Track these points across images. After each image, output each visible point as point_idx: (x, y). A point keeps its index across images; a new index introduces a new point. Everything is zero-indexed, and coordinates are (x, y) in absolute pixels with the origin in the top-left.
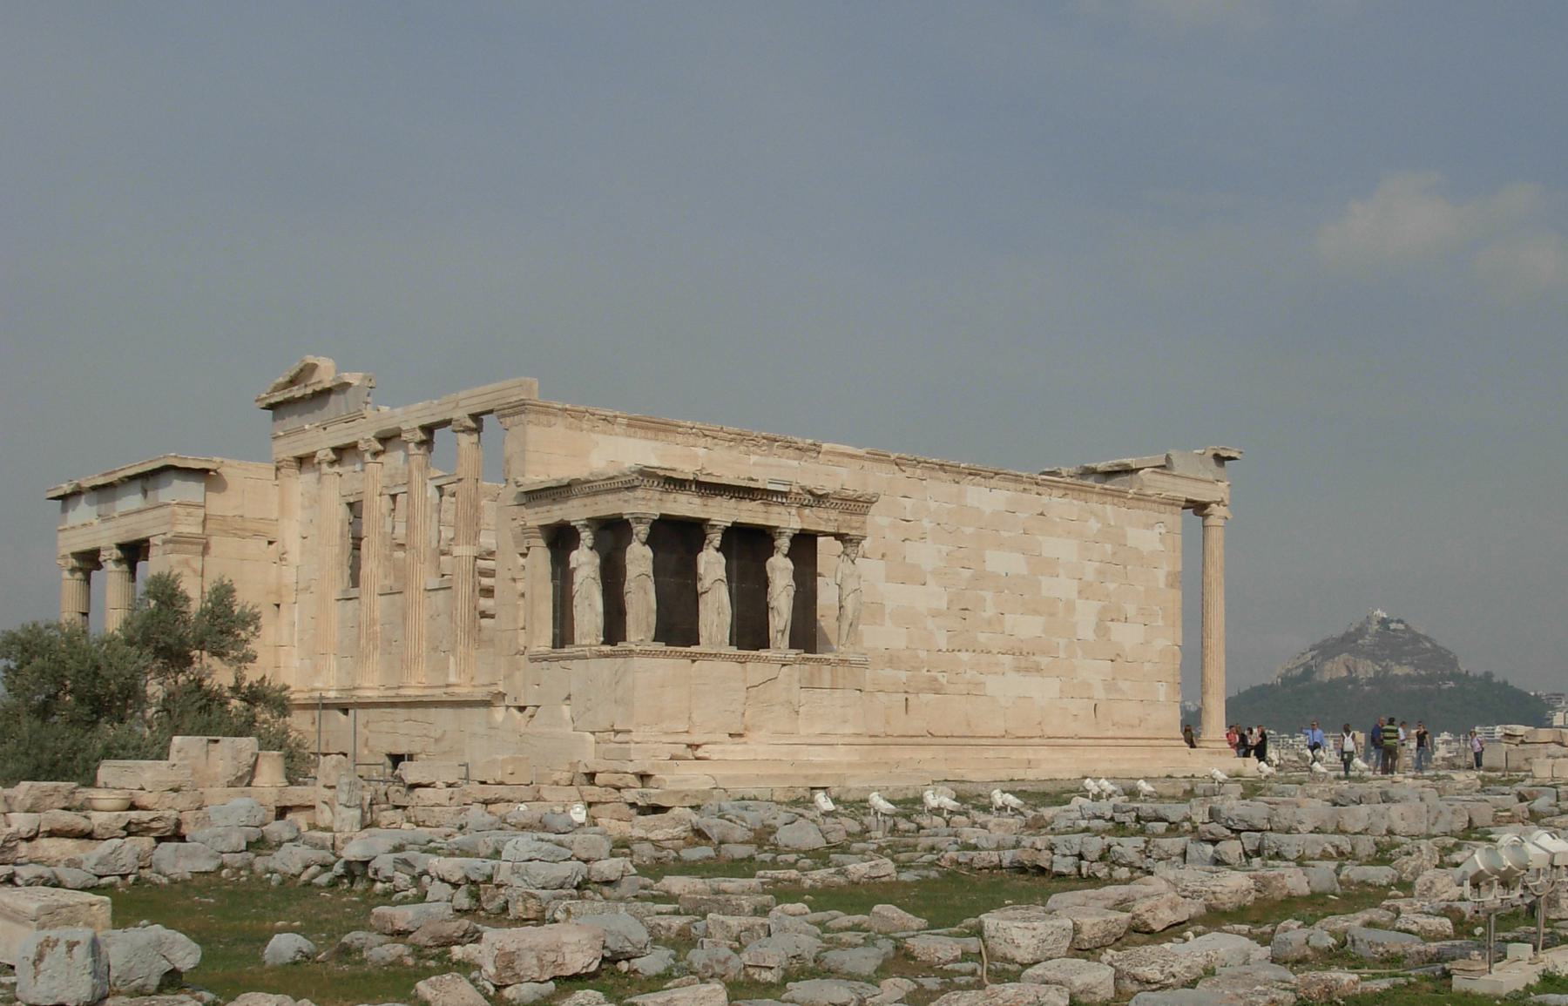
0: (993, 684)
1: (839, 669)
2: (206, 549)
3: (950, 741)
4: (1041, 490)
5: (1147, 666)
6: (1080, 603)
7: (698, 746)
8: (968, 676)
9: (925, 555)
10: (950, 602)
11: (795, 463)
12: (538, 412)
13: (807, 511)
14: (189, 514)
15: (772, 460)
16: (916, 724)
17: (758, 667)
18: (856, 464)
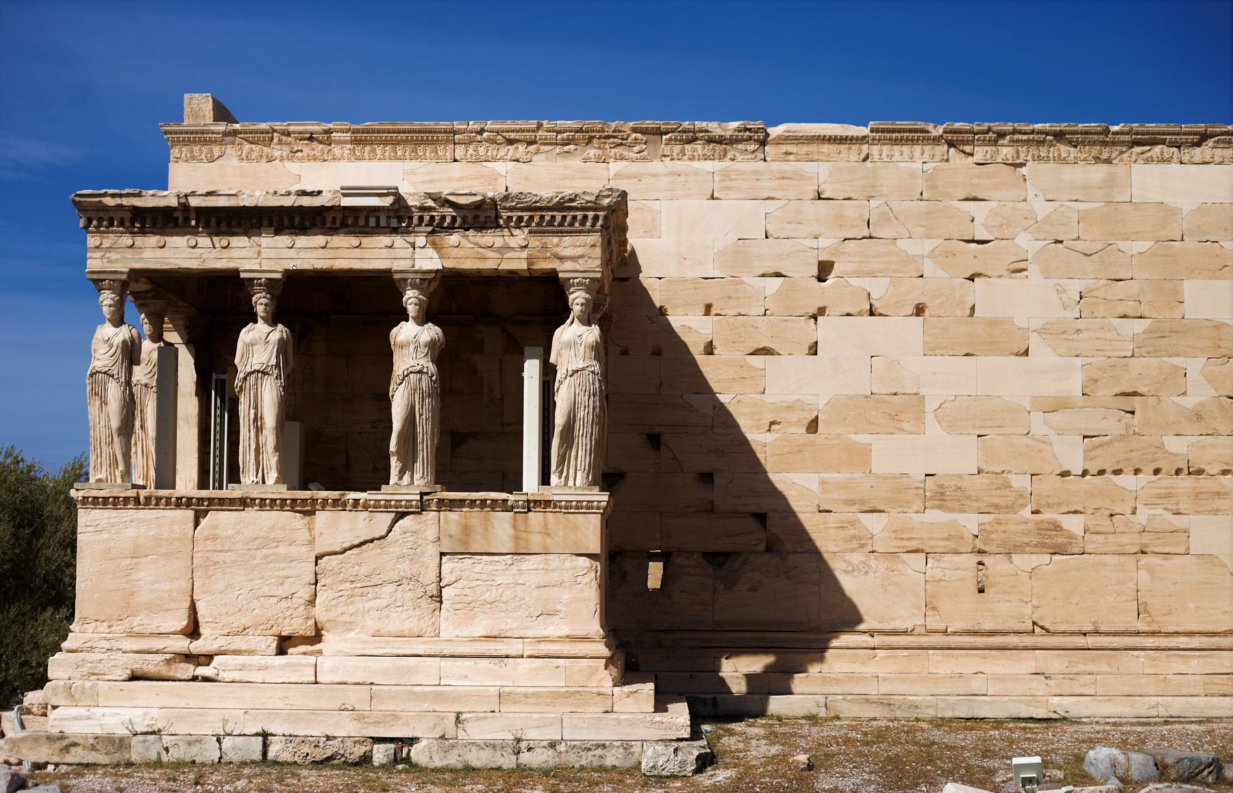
1: (535, 517)
3: (1090, 641)
9: (1026, 301)
11: (709, 165)
12: (188, 142)
13: (454, 238)
15: (656, 166)
16: (1002, 611)
18: (852, 154)
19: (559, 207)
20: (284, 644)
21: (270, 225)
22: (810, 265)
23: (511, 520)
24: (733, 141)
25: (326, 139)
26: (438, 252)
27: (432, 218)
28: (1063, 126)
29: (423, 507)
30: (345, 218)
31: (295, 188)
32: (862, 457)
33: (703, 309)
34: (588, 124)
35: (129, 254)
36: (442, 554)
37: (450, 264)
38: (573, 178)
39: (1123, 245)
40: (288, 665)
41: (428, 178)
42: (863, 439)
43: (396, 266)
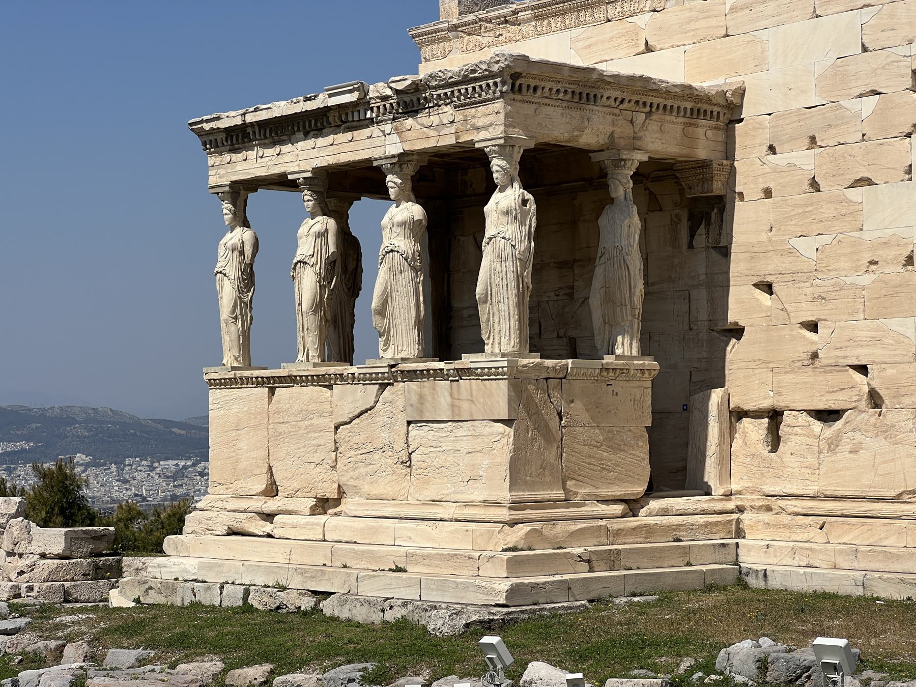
13: (409, 122)
19: (466, 80)
20: (323, 505)
21: (299, 130)
22: (903, 76)
23: (448, 388)
26: (400, 137)
27: (391, 104)
30: (340, 116)
33: (807, 141)
35: (229, 168)
36: (409, 423)
38: (697, 19)
40: (307, 524)
41: (588, 43)
43: (376, 153)
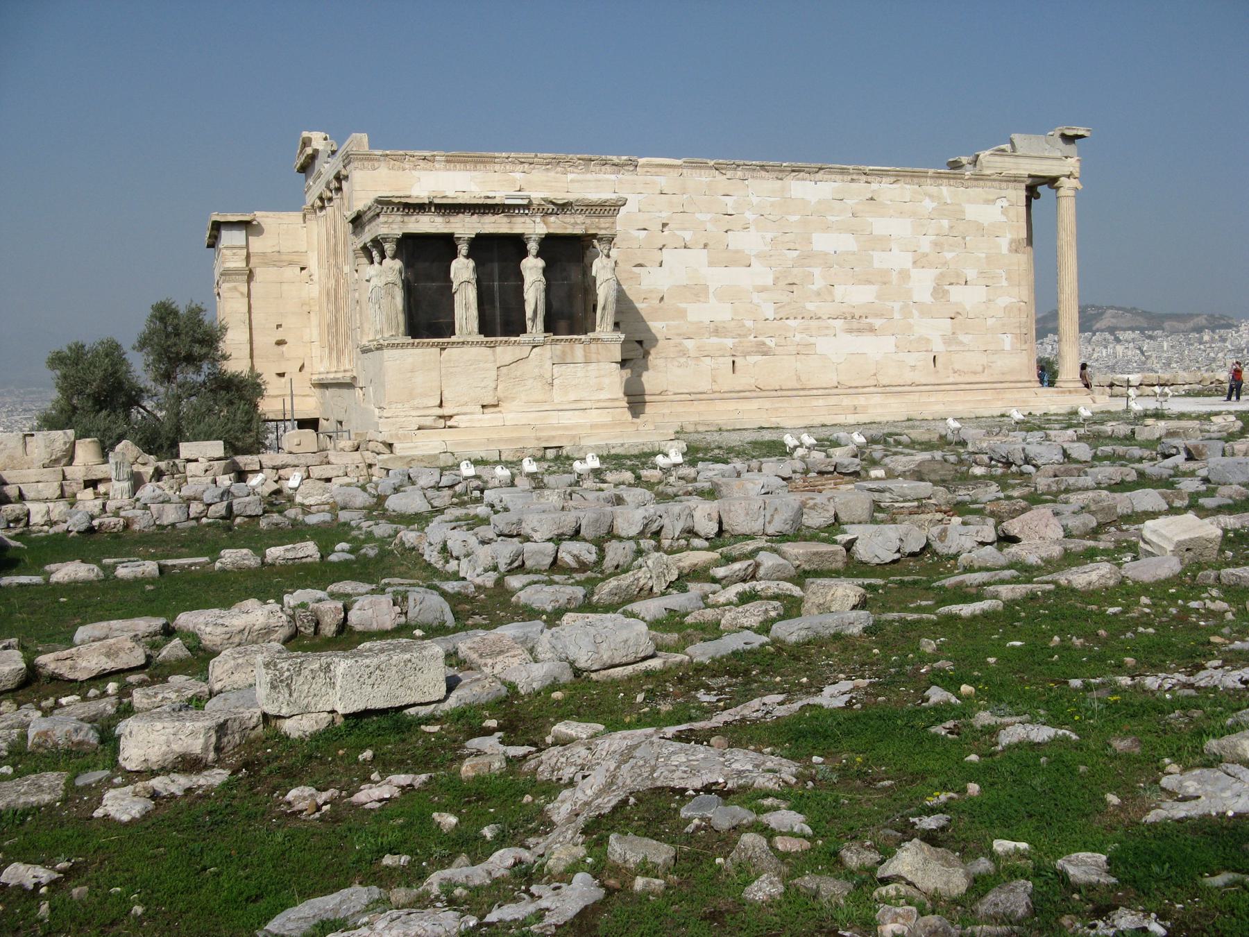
0: (824, 345)
1: (593, 346)
2: (250, 276)
3: (779, 393)
4: (870, 179)
5: (990, 322)
6: (915, 273)
7: (451, 417)
8: (798, 337)
9: (749, 241)
10: (776, 280)
11: (613, 177)
12: (361, 160)
13: (553, 219)
14: (234, 254)
15: (589, 176)
16: (743, 380)
17: (507, 350)
18: (674, 173)
24: (623, 165)
25: (431, 160)
28: (764, 163)
29: (544, 344)
31: (483, 195)
32: (682, 314)
34: (558, 155)
37: (551, 231)
39: (788, 217)
42: (683, 305)
